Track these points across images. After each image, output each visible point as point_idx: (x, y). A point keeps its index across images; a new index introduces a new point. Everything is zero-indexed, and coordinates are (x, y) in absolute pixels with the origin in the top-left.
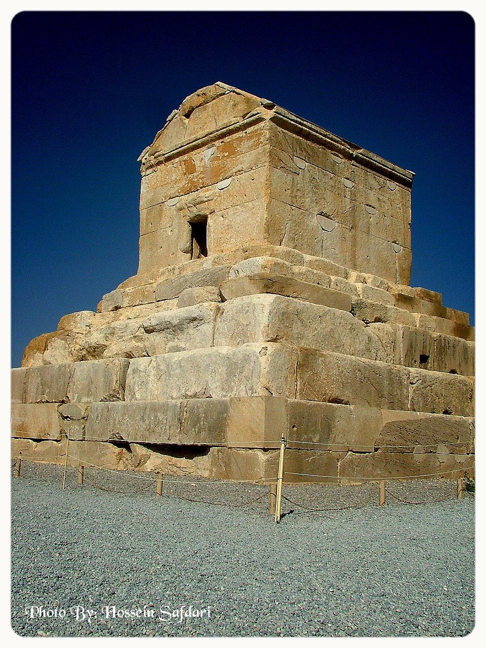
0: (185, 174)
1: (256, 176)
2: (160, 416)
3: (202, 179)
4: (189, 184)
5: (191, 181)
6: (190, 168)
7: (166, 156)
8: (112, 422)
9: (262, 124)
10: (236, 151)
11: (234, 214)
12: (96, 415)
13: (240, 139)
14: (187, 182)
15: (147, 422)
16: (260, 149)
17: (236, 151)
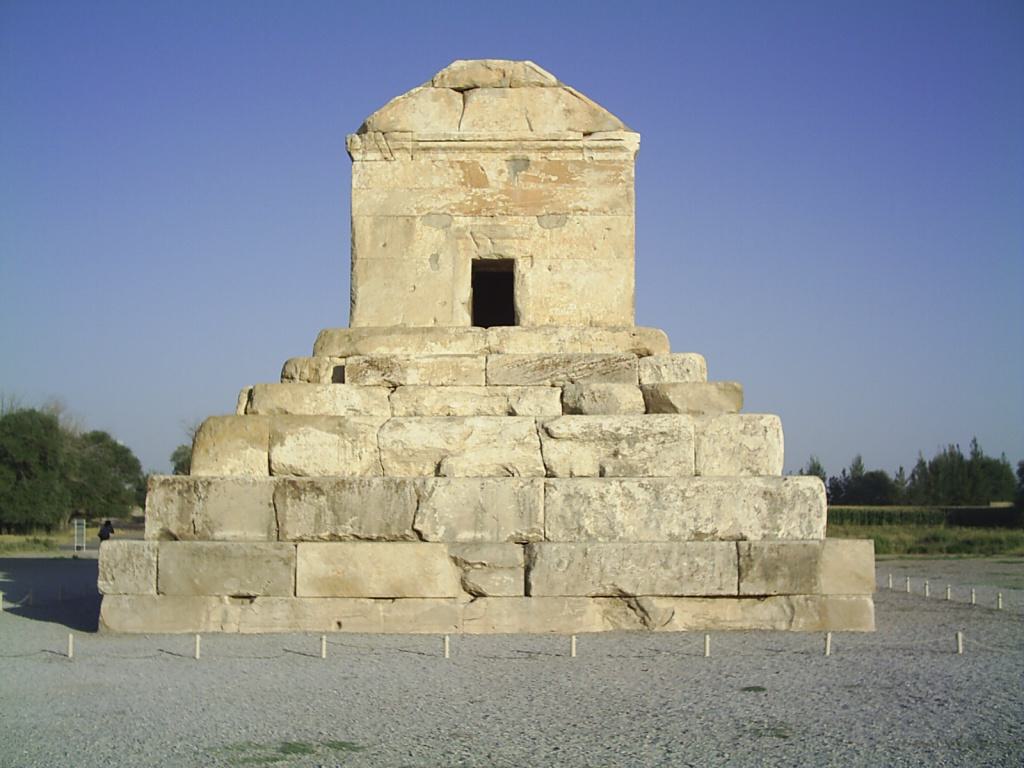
0: (463, 184)
1: (614, 226)
2: (700, 561)
3: (503, 201)
4: (475, 203)
5: (479, 199)
6: (474, 178)
7: (421, 144)
8: (596, 570)
9: (622, 156)
10: (574, 179)
11: (574, 270)
12: (556, 560)
13: (582, 164)
14: (470, 198)
15: (675, 569)
16: (620, 188)
17: (574, 179)
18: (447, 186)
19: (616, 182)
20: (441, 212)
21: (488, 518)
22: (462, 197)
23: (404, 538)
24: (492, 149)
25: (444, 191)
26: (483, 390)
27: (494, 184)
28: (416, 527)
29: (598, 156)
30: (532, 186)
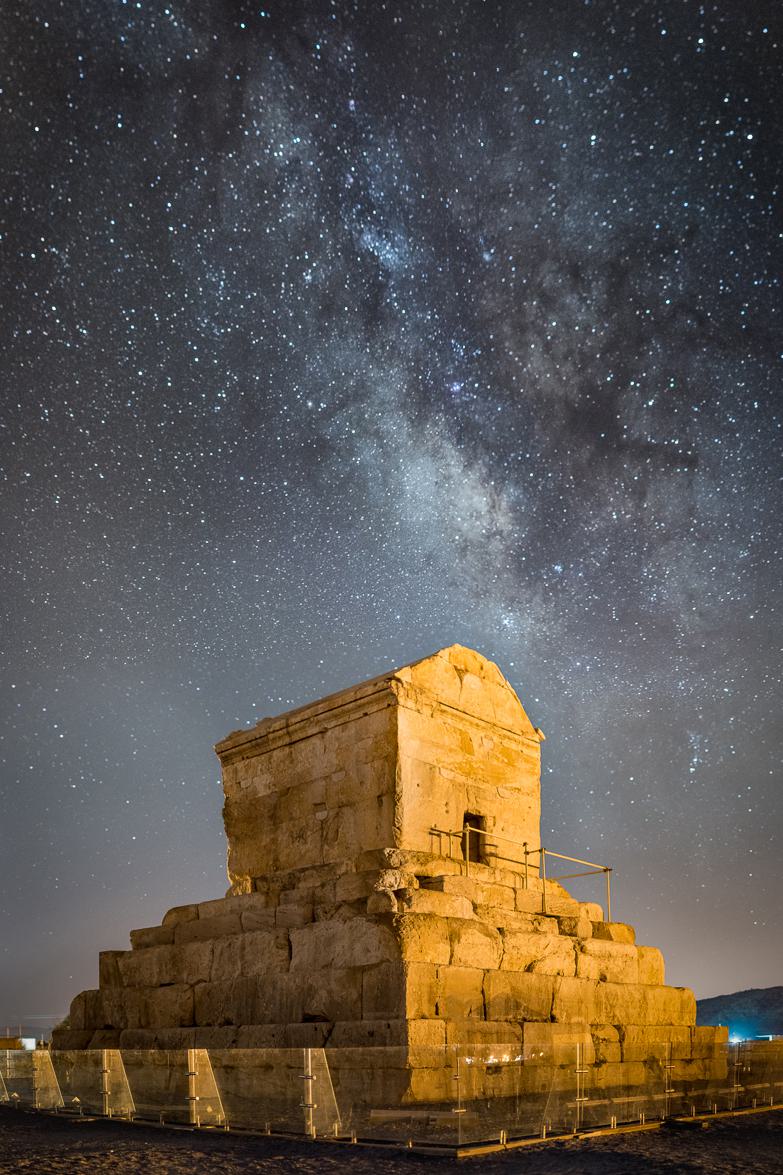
3: (483, 770)
5: (469, 763)
6: (466, 746)
18: (453, 747)
19: (533, 774)
20: (450, 767)
21: (583, 1009)
22: (459, 758)
23: (545, 1021)
24: (477, 725)
25: (451, 750)
26: (513, 914)
27: (476, 754)
28: (554, 1012)
29: (526, 751)
30: (495, 762)
